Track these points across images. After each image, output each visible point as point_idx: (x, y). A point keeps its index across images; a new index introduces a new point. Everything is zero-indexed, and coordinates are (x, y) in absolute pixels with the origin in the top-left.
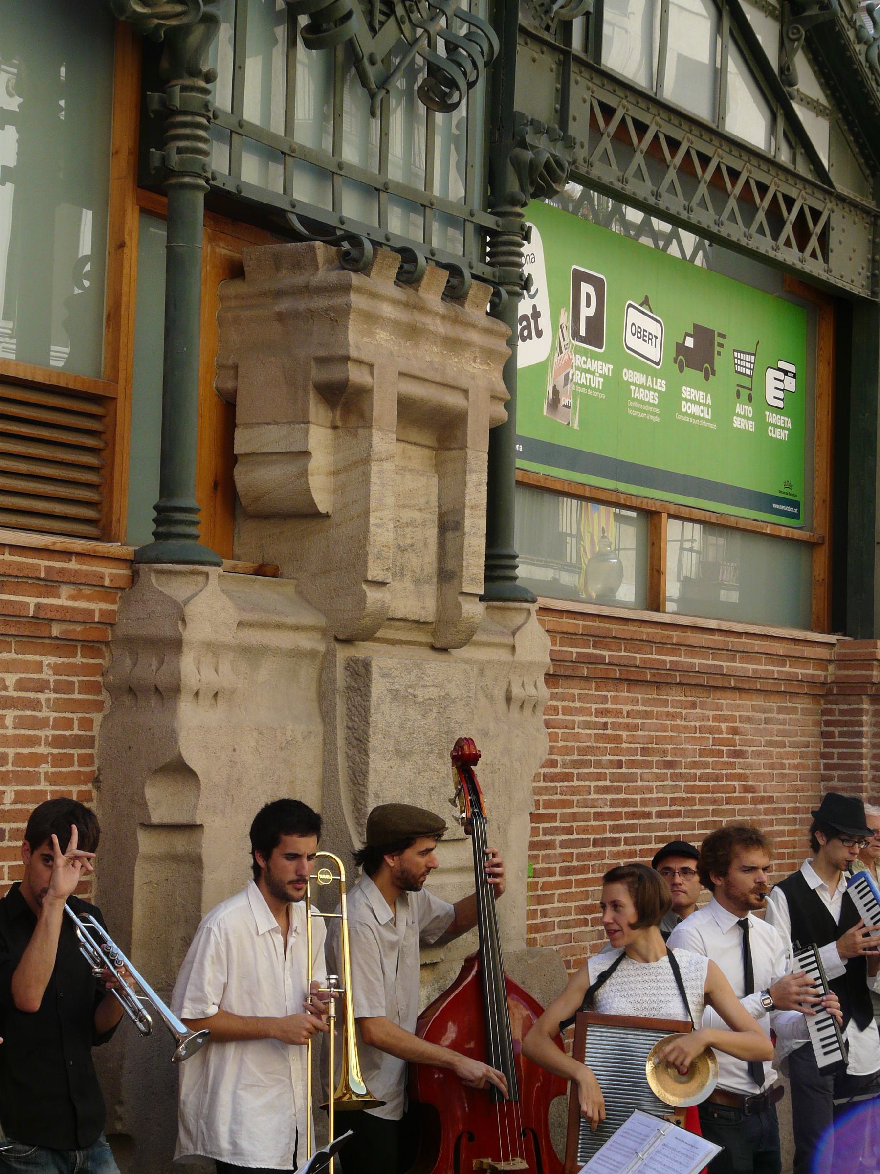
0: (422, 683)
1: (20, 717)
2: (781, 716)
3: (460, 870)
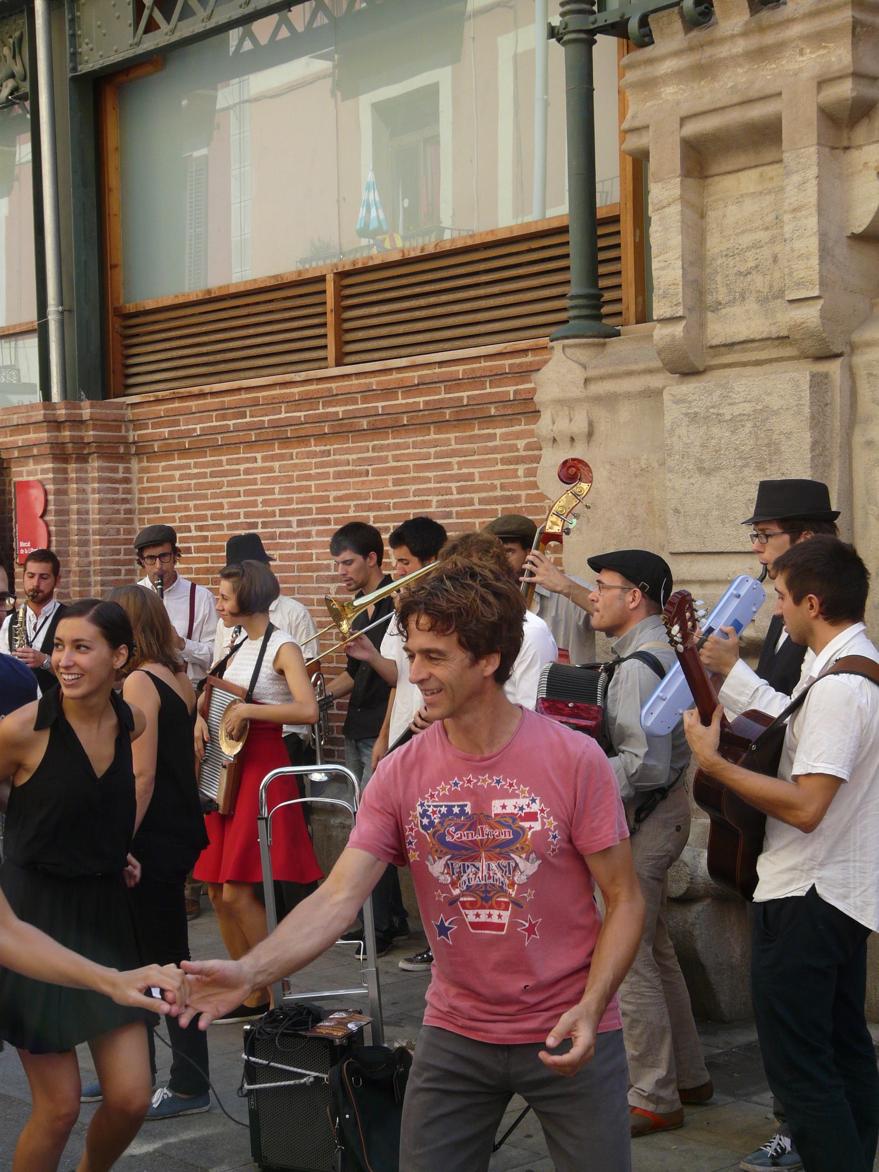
1: (528, 469)
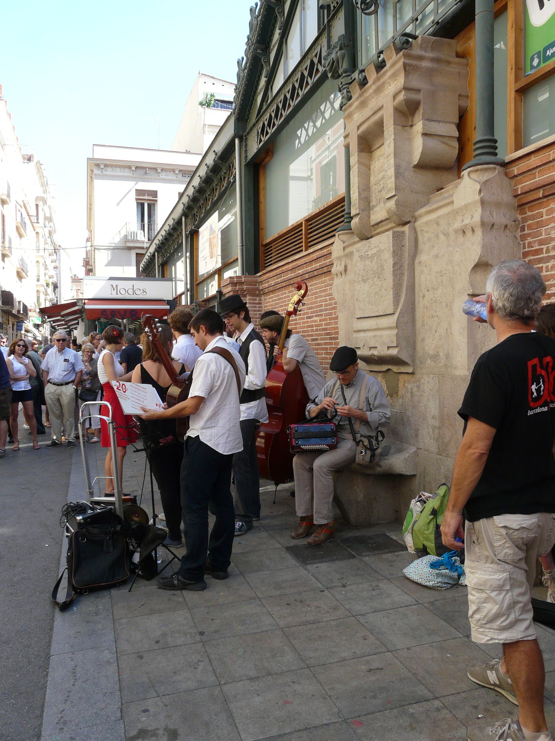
0: (370, 248)
3: (390, 328)
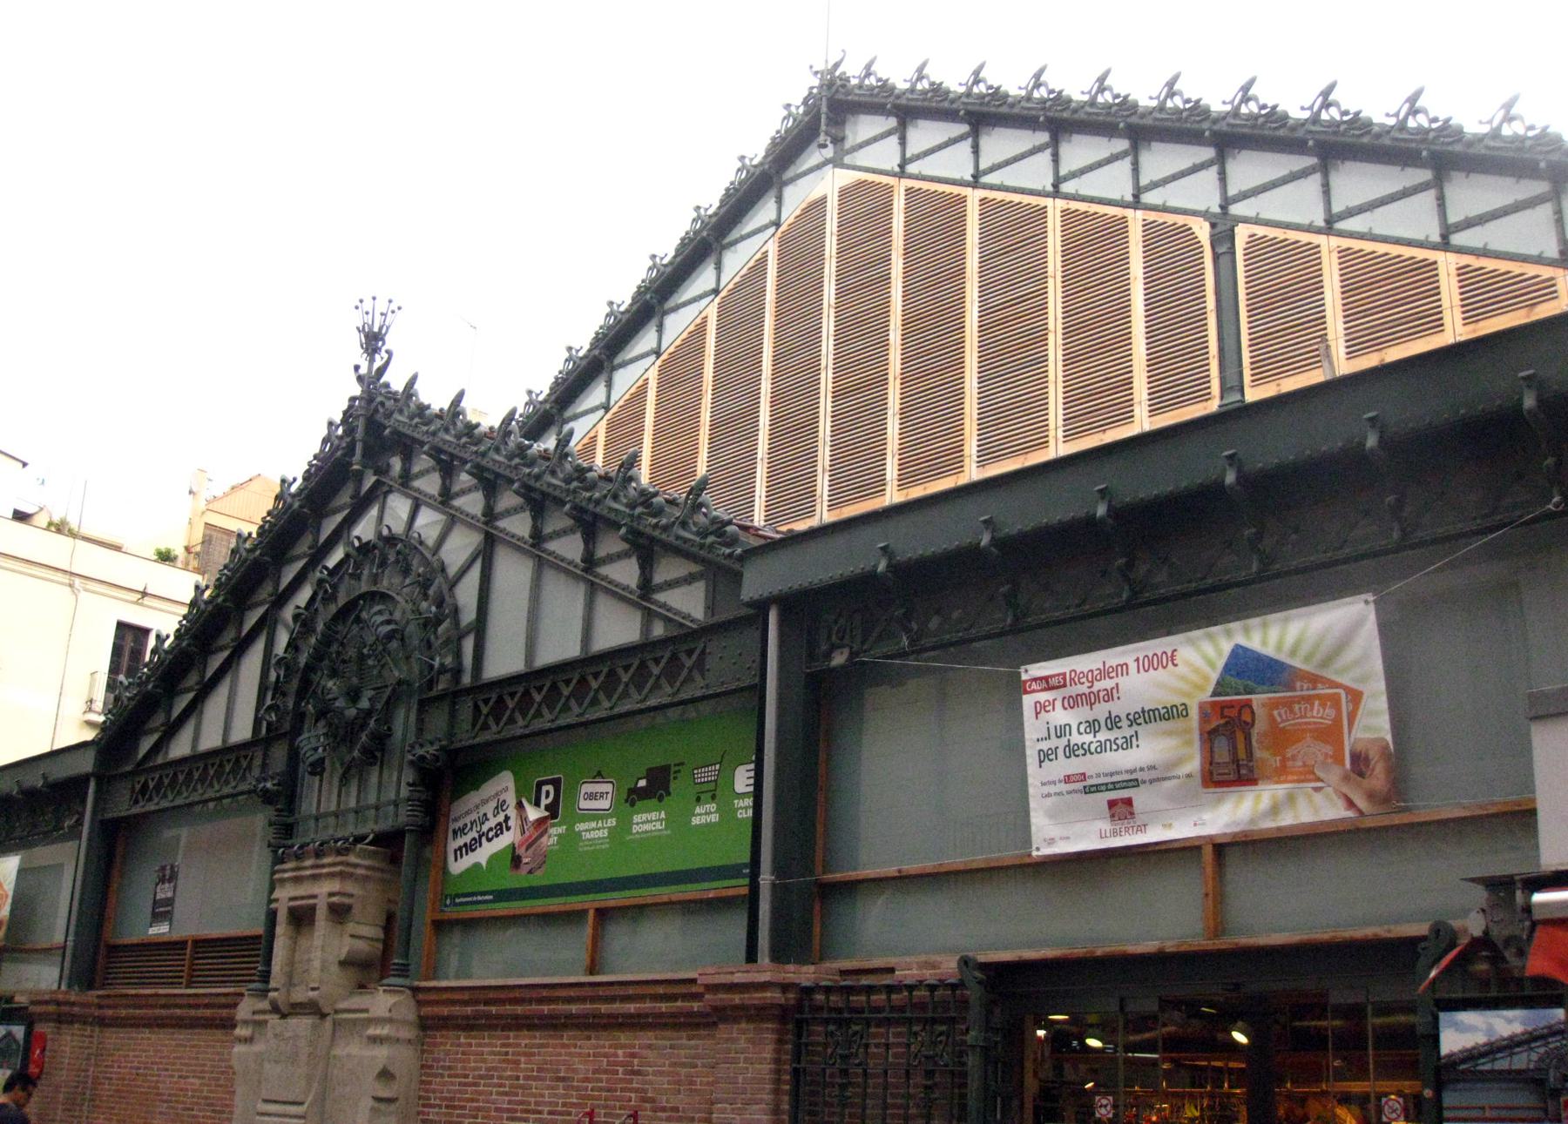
2: (692, 1042)
